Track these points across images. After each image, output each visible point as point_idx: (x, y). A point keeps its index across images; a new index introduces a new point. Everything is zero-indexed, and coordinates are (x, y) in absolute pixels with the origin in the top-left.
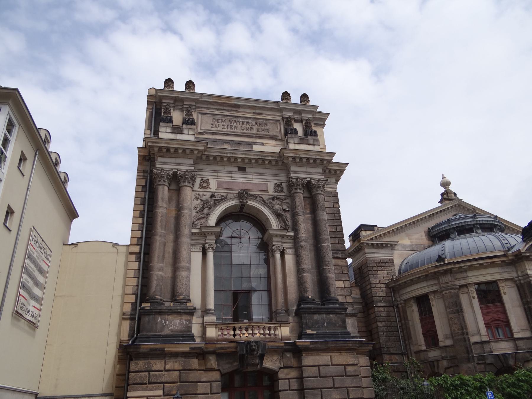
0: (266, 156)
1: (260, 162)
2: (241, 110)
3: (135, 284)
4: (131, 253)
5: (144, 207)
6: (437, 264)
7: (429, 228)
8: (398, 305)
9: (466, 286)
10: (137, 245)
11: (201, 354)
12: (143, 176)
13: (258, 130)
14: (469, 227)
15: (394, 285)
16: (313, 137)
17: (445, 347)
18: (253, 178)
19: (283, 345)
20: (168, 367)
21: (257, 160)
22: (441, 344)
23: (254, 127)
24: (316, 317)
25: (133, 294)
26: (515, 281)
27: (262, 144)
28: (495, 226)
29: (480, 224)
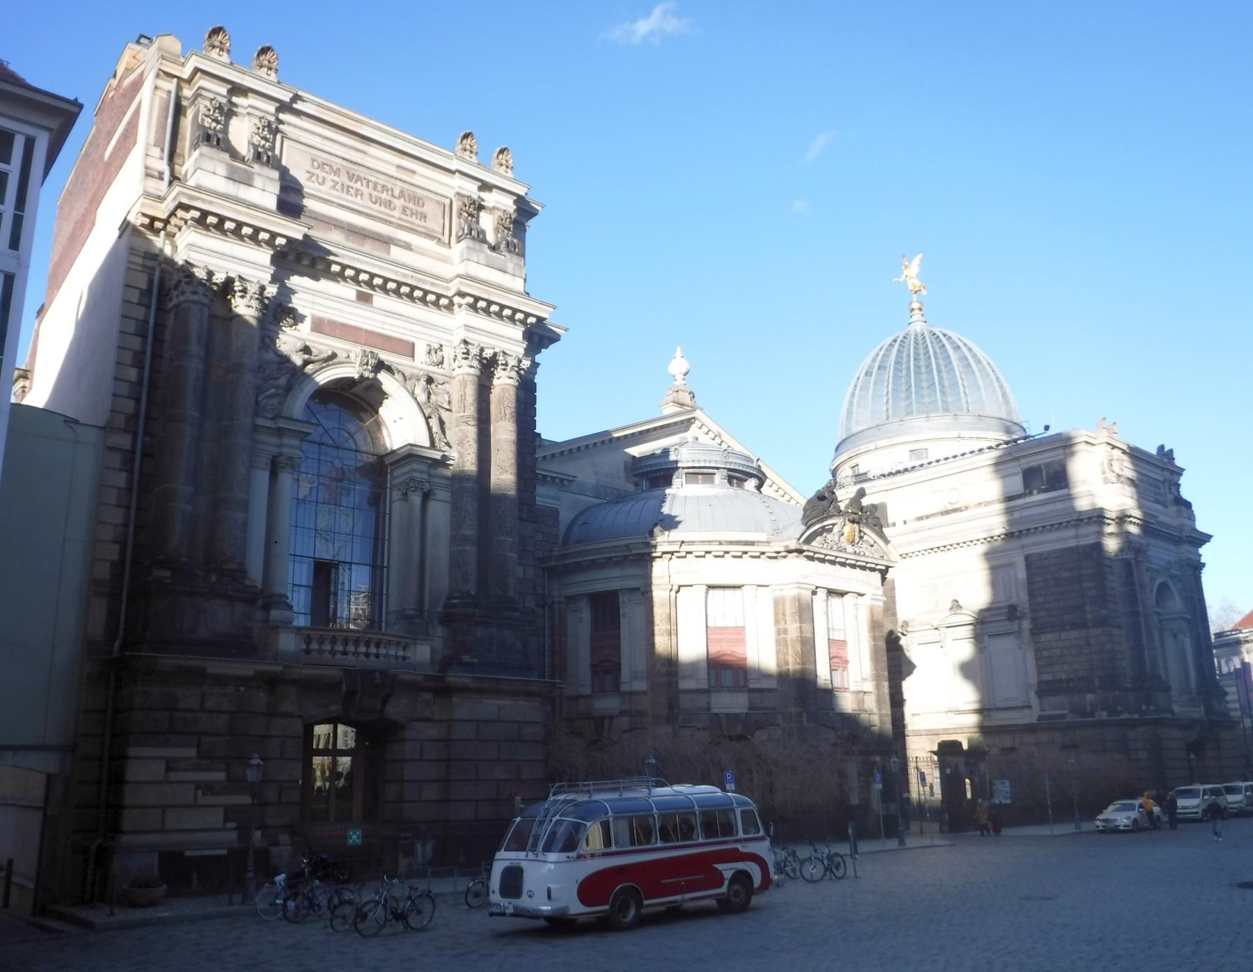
2: (373, 150)
3: (120, 521)
4: (111, 449)
5: (144, 343)
10: (125, 431)
11: (272, 682)
12: (144, 266)
13: (404, 209)
16: (515, 258)
17: (631, 693)
19: (420, 679)
20: (210, 704)
22: (624, 688)
23: (395, 200)
24: (480, 632)
25: (115, 542)
27: (408, 247)
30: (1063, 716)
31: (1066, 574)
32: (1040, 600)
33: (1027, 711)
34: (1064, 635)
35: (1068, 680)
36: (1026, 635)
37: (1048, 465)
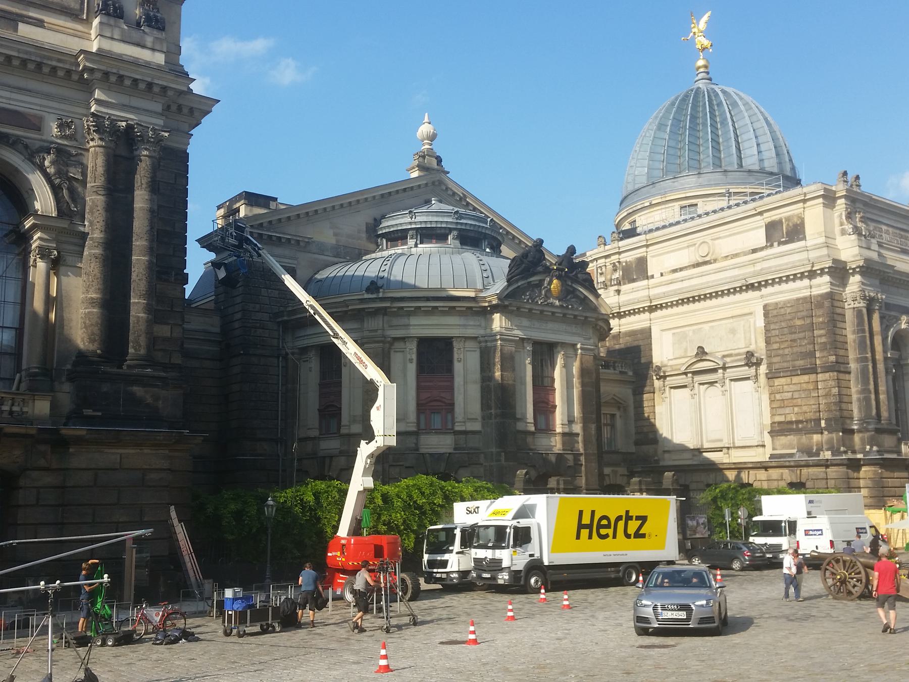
0: (45, 57)
1: (31, 66)
6: (366, 296)
7: (375, 220)
8: (287, 354)
9: (403, 339)
14: (443, 231)
15: (285, 318)
16: (156, 33)
18: (10, 99)
21: (24, 62)
22: (344, 431)
26: (480, 342)
27: (40, 24)
28: (485, 236)
29: (459, 230)
30: (791, 455)
31: (799, 323)
32: (776, 346)
33: (761, 449)
34: (796, 379)
35: (798, 422)
36: (762, 379)
37: (788, 219)
